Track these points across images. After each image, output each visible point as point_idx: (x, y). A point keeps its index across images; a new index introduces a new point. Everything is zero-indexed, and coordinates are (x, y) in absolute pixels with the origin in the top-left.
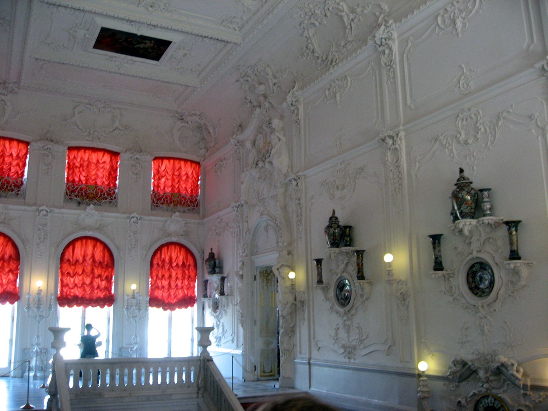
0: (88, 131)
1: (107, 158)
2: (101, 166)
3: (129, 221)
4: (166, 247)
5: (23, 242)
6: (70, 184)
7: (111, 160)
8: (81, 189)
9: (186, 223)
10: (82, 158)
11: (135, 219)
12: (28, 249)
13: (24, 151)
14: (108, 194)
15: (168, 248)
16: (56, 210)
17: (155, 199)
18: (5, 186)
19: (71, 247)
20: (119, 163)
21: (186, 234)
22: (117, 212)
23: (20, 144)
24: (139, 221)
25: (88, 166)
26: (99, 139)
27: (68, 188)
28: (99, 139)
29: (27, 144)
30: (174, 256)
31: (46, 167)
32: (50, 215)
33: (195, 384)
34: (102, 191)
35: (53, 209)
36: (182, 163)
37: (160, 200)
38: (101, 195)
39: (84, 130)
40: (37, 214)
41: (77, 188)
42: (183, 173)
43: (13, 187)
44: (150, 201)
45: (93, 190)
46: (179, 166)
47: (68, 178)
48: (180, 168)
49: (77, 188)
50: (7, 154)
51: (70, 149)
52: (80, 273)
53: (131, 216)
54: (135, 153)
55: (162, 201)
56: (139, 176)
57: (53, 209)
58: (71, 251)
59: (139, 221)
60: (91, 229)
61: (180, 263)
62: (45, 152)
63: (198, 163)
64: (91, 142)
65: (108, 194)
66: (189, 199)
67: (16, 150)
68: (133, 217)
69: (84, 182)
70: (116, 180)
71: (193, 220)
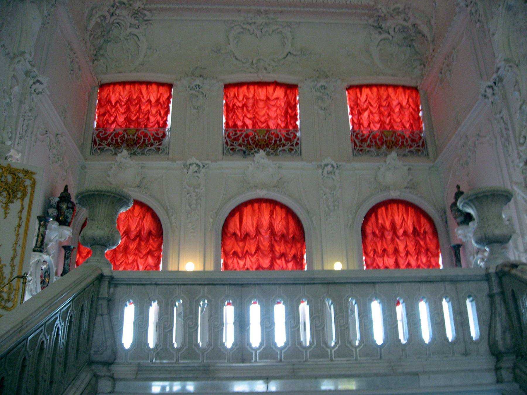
0: (250, 61)
1: (279, 93)
2: (273, 103)
3: (320, 171)
4: (383, 208)
5: (167, 211)
6: (231, 130)
7: (286, 94)
8: (247, 136)
9: (409, 169)
10: (244, 96)
11: (329, 168)
12: (173, 222)
13: (166, 96)
14: (287, 139)
15: (387, 209)
17: (356, 141)
18: (142, 141)
19: (237, 215)
20: (298, 98)
21: (412, 186)
22: (302, 160)
23: (161, 88)
24: (337, 172)
25: (254, 105)
26: (266, 69)
27: (229, 136)
28: (266, 69)
29: (170, 86)
30: (398, 219)
32: (203, 171)
33: (484, 347)
34: (277, 136)
35: (206, 162)
36: (391, 90)
37: (365, 143)
38: (276, 141)
39: (244, 61)
40: (185, 170)
42: (395, 103)
43: (152, 141)
44: (350, 145)
45: (264, 136)
46: (386, 93)
47: (227, 123)
48: (388, 96)
49: (242, 134)
50: (144, 101)
51: (227, 87)
52: (253, 253)
55: (368, 142)
57: (206, 162)
58: (238, 221)
59: (337, 172)
60: (264, 186)
61: (410, 230)
62: (193, 92)
63: (415, 89)
64: (256, 75)
65: (287, 139)
66: (409, 137)
67: (155, 95)
68: (326, 165)
69: (250, 127)
70: (297, 119)
71: (419, 164)
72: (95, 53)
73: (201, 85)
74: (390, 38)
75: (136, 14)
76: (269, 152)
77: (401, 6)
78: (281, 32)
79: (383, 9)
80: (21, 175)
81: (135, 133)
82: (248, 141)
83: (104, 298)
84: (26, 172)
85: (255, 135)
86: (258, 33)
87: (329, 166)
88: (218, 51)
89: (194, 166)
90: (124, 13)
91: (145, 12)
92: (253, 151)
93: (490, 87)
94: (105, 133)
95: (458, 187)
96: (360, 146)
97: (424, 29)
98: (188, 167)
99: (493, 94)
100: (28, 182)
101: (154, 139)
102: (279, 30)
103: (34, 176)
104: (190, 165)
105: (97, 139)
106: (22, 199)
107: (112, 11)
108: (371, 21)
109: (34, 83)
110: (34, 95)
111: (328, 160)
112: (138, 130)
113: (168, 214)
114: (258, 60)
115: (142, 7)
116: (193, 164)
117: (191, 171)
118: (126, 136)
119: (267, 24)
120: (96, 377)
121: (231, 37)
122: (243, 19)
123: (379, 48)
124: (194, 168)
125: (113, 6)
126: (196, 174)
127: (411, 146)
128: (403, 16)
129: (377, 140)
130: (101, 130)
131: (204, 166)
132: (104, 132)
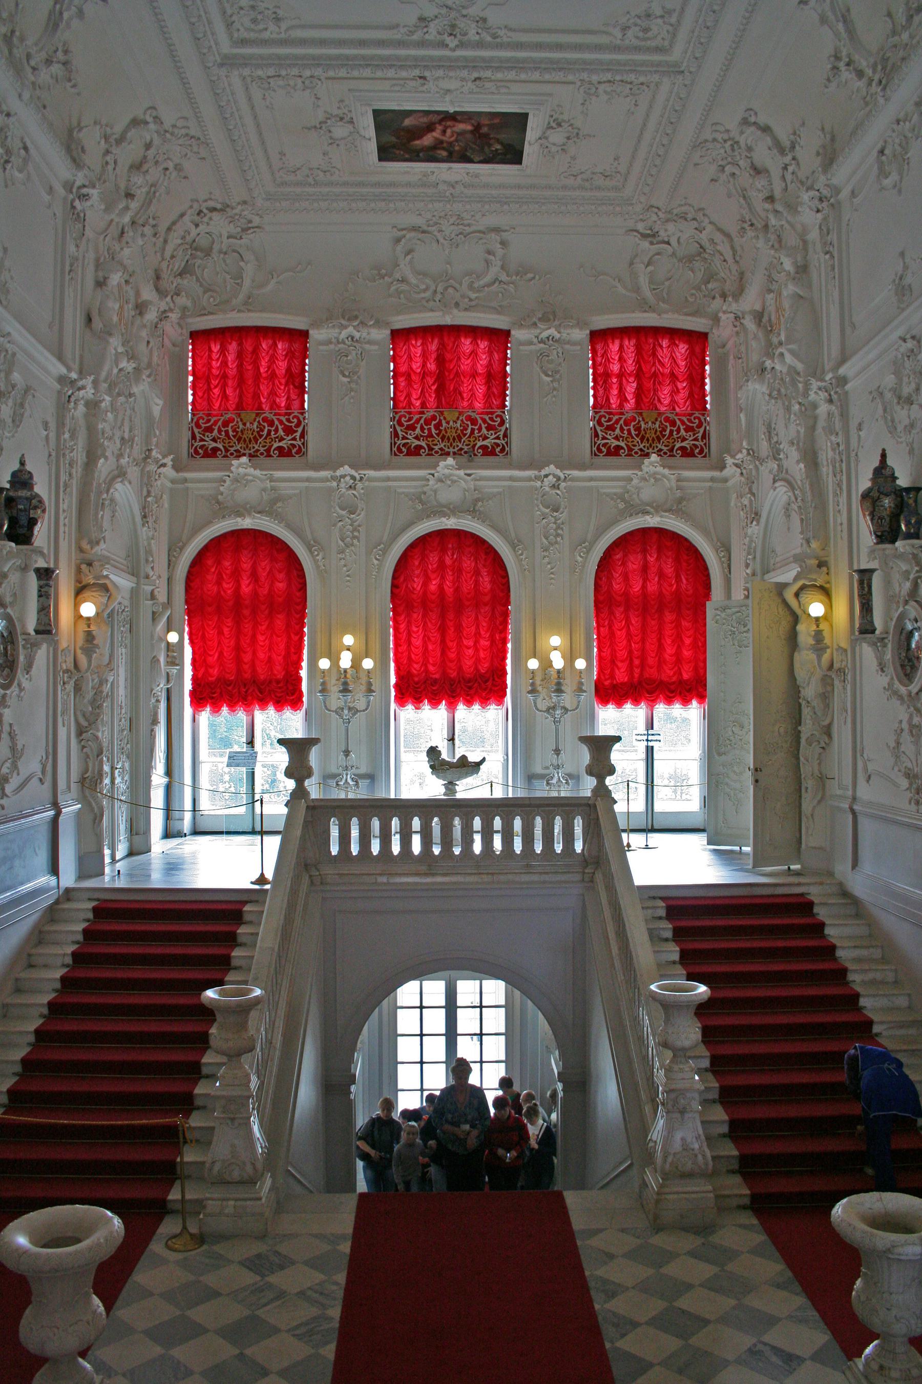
12: (321, 564)
14: (489, 428)
16: (372, 473)
22: (510, 466)
29: (303, 335)
31: (346, 380)
32: (359, 485)
51: (397, 335)
53: (543, 473)
54: (542, 327)
56: (558, 376)
68: (546, 476)
81: (255, 420)
82: (429, 430)
85: (440, 420)
87: (551, 477)
89: (348, 478)
96: (604, 438)
112: (257, 414)
114: (446, 289)
116: (345, 476)
117: (342, 485)
118: (241, 426)
127: (684, 440)
129: (632, 427)
130: (201, 414)
131: (361, 478)
132: (206, 418)
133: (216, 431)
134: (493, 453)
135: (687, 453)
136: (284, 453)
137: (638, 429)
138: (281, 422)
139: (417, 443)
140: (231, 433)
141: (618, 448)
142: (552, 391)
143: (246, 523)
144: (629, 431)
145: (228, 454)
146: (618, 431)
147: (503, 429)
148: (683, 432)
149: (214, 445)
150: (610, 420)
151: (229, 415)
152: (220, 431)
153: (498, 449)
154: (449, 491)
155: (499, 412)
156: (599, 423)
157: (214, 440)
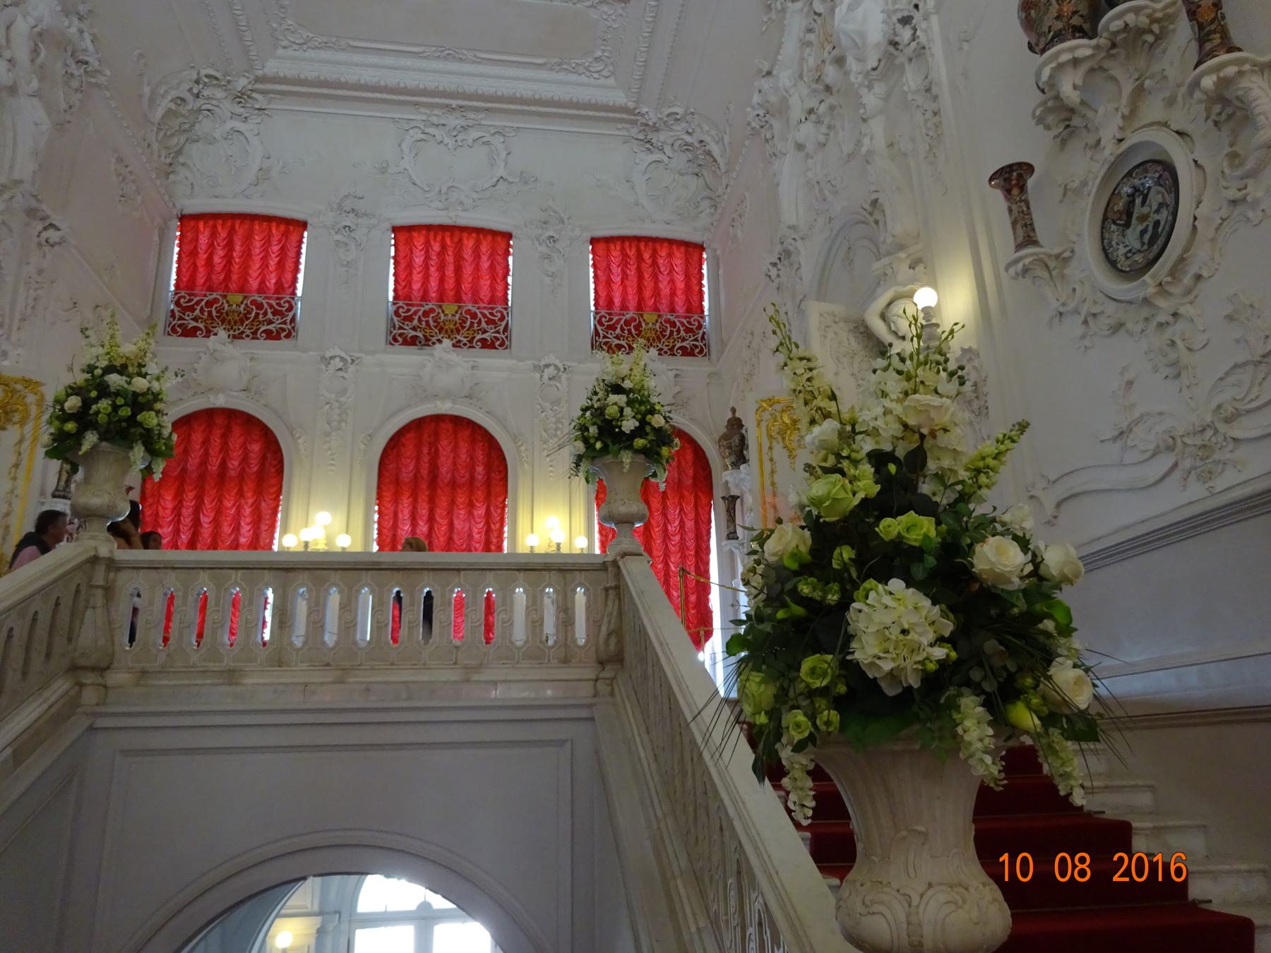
3: (538, 375)
9: (676, 376)
11: (551, 371)
14: (489, 322)
17: (599, 328)
24: (564, 376)
27: (397, 313)
28: (461, 203)
32: (352, 368)
40: (323, 367)
41: (416, 313)
43: (270, 316)
59: (564, 376)
62: (337, 237)
64: (444, 213)
68: (547, 366)
72: (168, 161)
73: (353, 227)
74: (666, 160)
75: (241, 97)
76: (459, 341)
77: (680, 110)
78: (487, 143)
79: (652, 115)
80: (19, 387)
83: (98, 587)
84: (28, 383)
86: (451, 142)
87: (552, 368)
88: (383, 171)
89: (338, 359)
90: (220, 94)
91: (254, 95)
92: (434, 339)
93: (775, 265)
94: (190, 301)
95: (734, 410)
96: (605, 337)
97: (716, 151)
98: (327, 361)
99: (778, 276)
100: (31, 399)
101: (275, 313)
102: (484, 140)
103: (42, 389)
104: (332, 358)
105: (176, 309)
106: (22, 423)
107: (195, 91)
108: (634, 131)
109: (45, 229)
110: (47, 248)
111: (551, 359)
112: (245, 297)
113: (293, 435)
115: (250, 87)
117: (332, 368)
118: (226, 305)
119: (465, 128)
120: (81, 685)
121: (405, 147)
122: (424, 118)
123: (647, 176)
124: (337, 363)
125: (197, 82)
126: (341, 374)
127: (684, 340)
128: (684, 125)
130: (183, 293)
133: (197, 312)
134: (492, 346)
135: (686, 352)
136: (270, 335)
137: (638, 327)
138: (271, 306)
139: (414, 333)
140: (214, 314)
141: (619, 347)
142: (553, 292)
143: (220, 401)
144: (629, 331)
145: (208, 333)
146: (618, 331)
147: (504, 323)
148: (683, 333)
149: (193, 324)
150: (611, 320)
151: (215, 295)
152: (202, 311)
153: (497, 343)
154: (445, 378)
155: (500, 308)
156: (600, 323)
157: (195, 319)
